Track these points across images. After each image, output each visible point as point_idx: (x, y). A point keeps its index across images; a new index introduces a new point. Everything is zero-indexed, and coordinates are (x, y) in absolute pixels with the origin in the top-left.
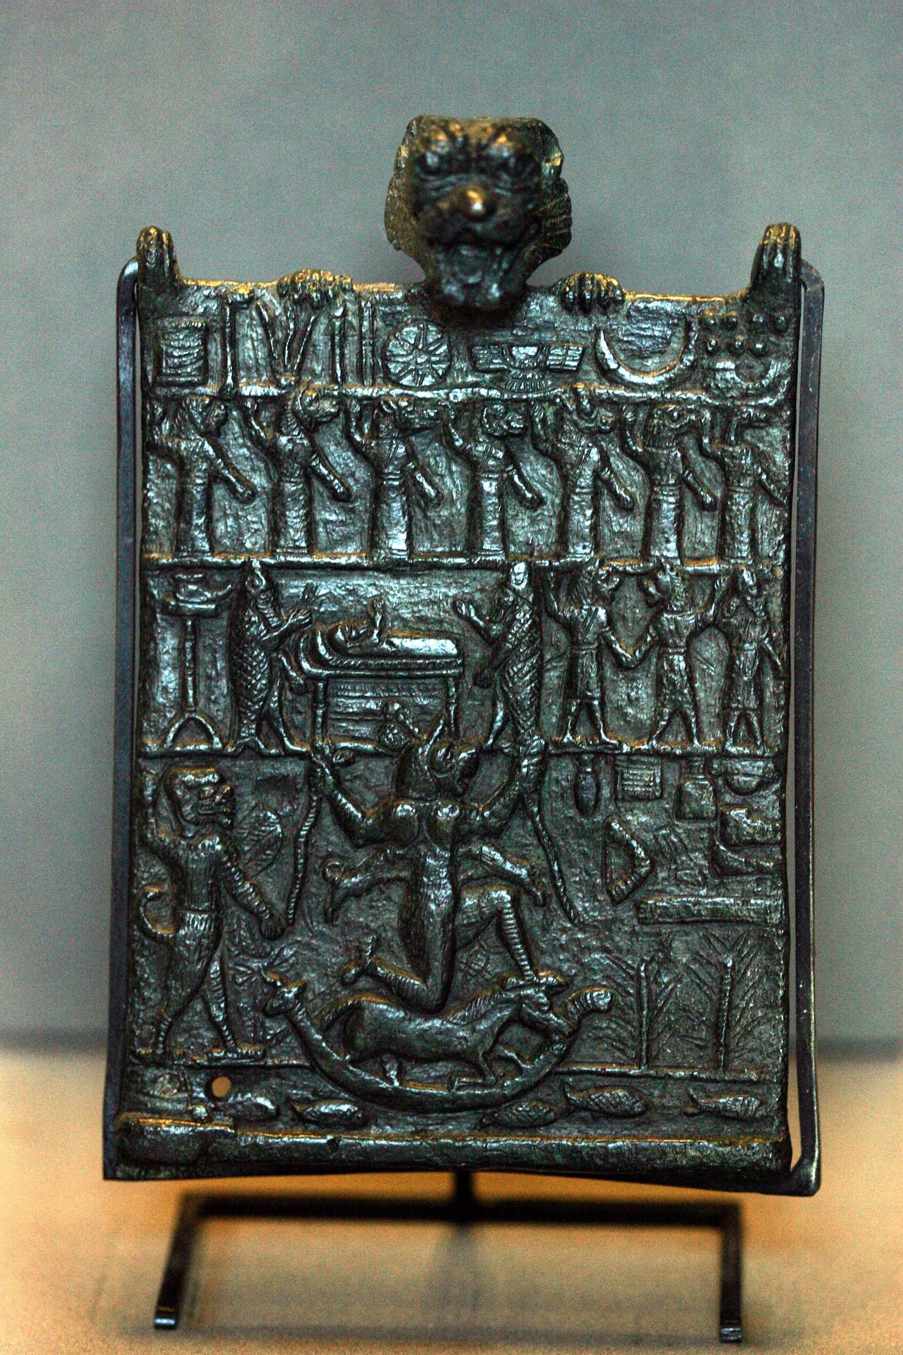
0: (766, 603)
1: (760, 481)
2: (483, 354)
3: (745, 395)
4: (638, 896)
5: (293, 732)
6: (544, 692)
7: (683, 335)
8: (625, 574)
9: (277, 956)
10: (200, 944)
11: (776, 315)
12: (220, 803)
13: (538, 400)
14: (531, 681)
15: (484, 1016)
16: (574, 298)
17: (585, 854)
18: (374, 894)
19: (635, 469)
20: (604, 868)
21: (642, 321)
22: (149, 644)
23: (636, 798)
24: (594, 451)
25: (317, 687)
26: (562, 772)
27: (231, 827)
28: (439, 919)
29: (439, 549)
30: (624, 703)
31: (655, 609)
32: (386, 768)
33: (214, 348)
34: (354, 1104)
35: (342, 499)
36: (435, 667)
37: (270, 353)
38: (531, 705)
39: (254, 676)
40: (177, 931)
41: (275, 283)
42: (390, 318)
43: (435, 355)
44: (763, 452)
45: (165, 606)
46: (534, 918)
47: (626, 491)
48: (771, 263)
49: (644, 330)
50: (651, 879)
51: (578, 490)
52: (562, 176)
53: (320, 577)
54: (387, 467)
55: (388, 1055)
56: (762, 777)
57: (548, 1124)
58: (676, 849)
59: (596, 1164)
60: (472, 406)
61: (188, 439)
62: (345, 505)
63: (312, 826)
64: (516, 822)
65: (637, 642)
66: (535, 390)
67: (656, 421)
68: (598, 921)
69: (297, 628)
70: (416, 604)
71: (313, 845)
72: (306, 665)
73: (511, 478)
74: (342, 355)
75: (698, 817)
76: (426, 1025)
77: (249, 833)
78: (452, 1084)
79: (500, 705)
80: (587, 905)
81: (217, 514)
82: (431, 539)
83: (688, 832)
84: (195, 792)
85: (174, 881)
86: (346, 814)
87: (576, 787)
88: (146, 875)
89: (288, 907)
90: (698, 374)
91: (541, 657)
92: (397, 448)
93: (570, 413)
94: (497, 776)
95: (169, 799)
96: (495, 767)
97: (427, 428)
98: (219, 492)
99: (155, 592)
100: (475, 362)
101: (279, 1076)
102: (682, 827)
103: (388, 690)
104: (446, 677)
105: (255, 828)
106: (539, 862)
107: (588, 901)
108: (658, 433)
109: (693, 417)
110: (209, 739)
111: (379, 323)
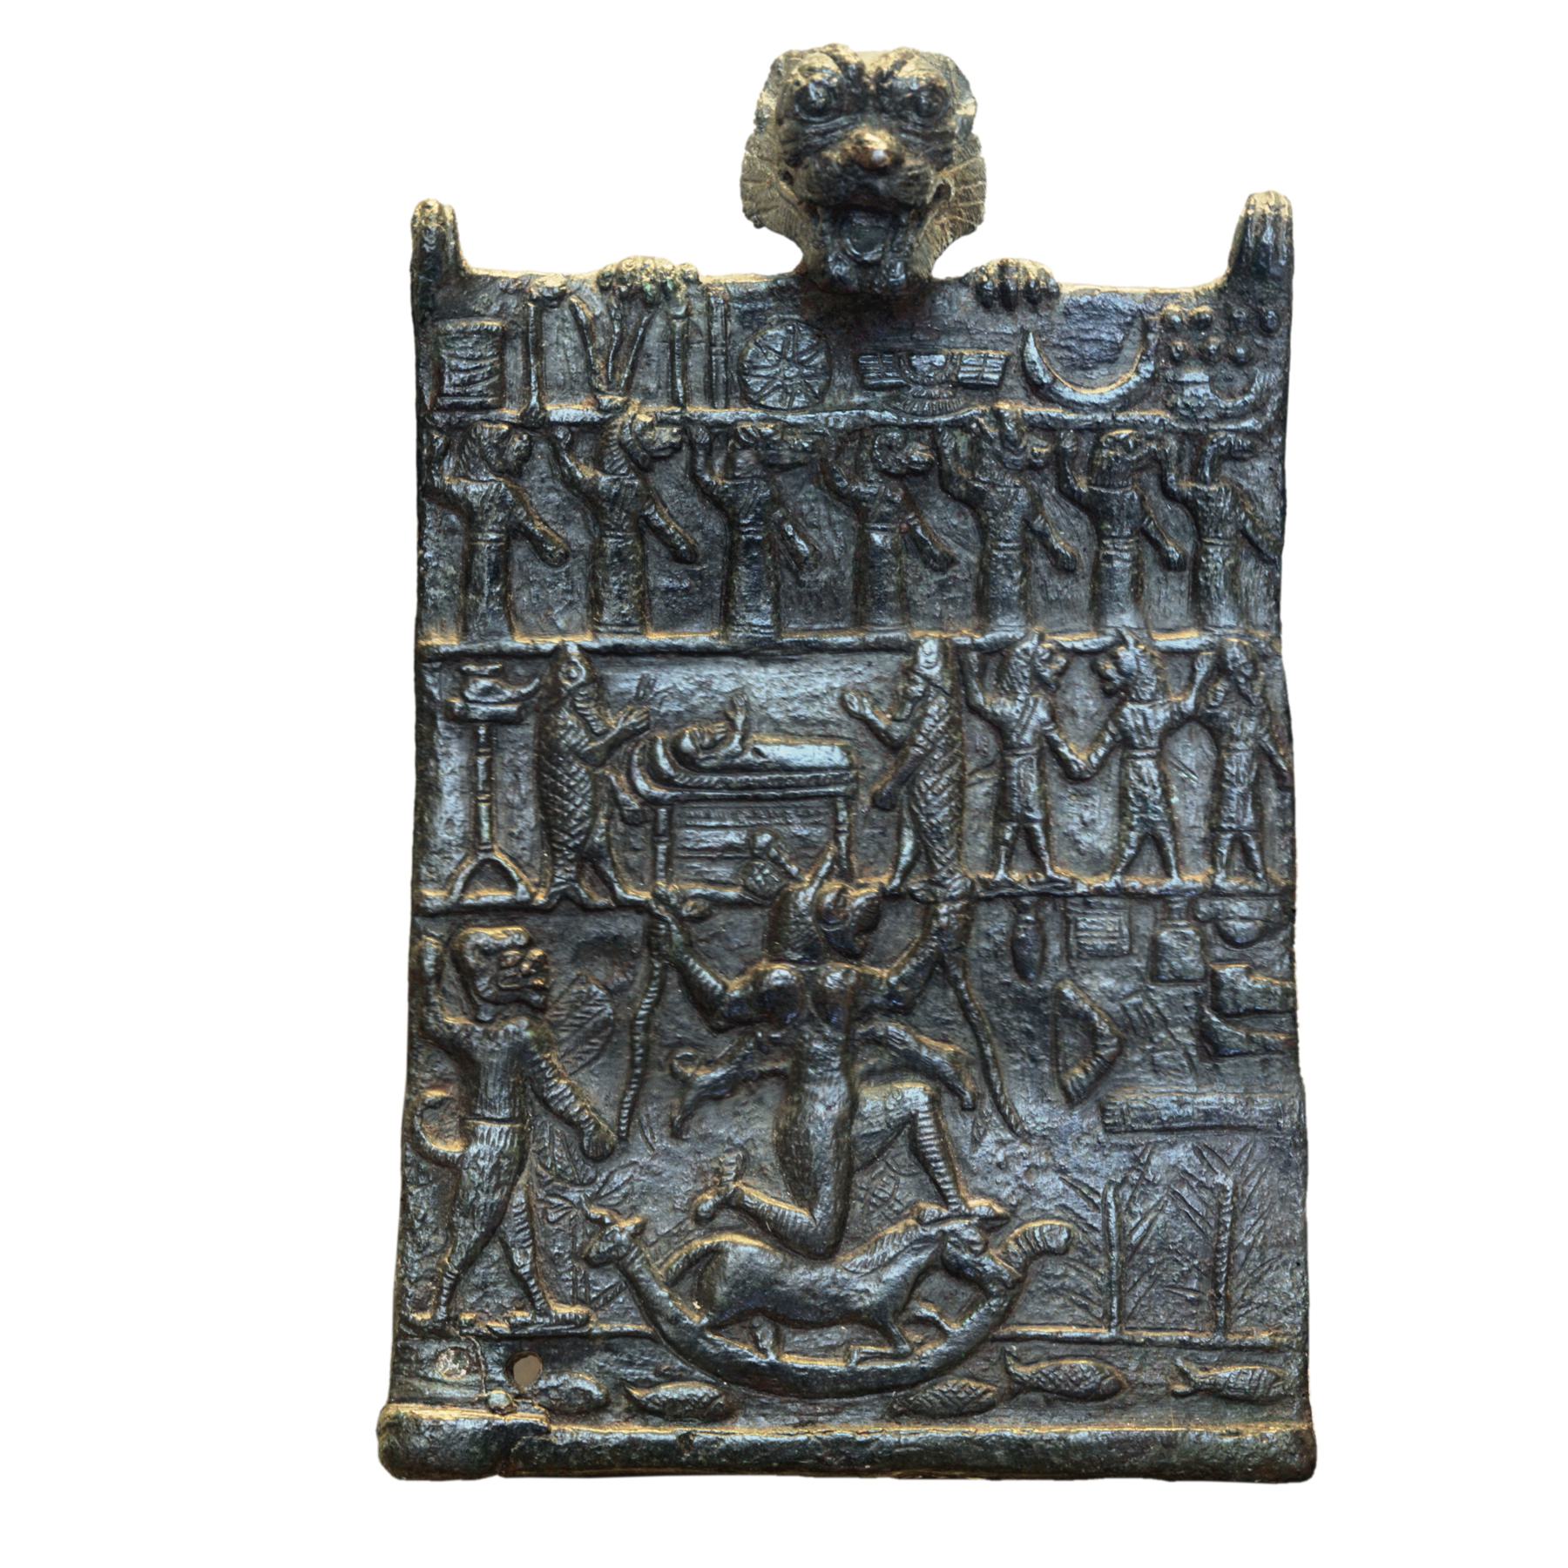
2: (873, 368)
3: (1223, 417)
4: (1102, 1092)
6: (966, 815)
7: (1138, 338)
8: (1076, 652)
9: (605, 1182)
10: (497, 1166)
12: (528, 975)
13: (946, 424)
14: (950, 799)
15: (893, 1260)
17: (1028, 1033)
18: (742, 1095)
20: (1054, 1050)
21: (1083, 321)
22: (426, 761)
23: (1098, 955)
24: (1022, 492)
25: (656, 814)
26: (995, 923)
28: (830, 1126)
29: (817, 626)
30: (1075, 828)
31: (1115, 699)
32: (755, 921)
33: (514, 359)
34: (715, 1385)
36: (819, 783)
38: (951, 832)
39: (571, 801)
42: (748, 318)
43: (808, 367)
46: (959, 1127)
49: (1087, 331)
53: (660, 666)
55: (761, 1319)
56: (1265, 921)
58: (1152, 1022)
59: (1052, 1463)
60: (860, 432)
62: (689, 568)
63: (657, 1003)
64: (935, 990)
66: (943, 412)
69: (630, 735)
70: (791, 700)
71: (656, 1029)
72: (642, 785)
74: (685, 369)
75: (1179, 979)
76: (815, 1275)
77: (568, 1016)
78: (850, 1357)
79: (908, 833)
83: (1169, 1000)
84: (494, 960)
86: (701, 985)
87: (1015, 943)
89: (620, 1117)
90: (1157, 388)
91: (963, 768)
93: (991, 441)
94: (905, 930)
95: (458, 969)
96: (903, 918)
97: (800, 464)
98: (520, 552)
99: (435, 691)
100: (863, 378)
101: (608, 1349)
102: (1162, 994)
103: (755, 816)
104: (836, 795)
105: (577, 1008)
108: (1109, 468)
110: (512, 885)
111: (733, 325)
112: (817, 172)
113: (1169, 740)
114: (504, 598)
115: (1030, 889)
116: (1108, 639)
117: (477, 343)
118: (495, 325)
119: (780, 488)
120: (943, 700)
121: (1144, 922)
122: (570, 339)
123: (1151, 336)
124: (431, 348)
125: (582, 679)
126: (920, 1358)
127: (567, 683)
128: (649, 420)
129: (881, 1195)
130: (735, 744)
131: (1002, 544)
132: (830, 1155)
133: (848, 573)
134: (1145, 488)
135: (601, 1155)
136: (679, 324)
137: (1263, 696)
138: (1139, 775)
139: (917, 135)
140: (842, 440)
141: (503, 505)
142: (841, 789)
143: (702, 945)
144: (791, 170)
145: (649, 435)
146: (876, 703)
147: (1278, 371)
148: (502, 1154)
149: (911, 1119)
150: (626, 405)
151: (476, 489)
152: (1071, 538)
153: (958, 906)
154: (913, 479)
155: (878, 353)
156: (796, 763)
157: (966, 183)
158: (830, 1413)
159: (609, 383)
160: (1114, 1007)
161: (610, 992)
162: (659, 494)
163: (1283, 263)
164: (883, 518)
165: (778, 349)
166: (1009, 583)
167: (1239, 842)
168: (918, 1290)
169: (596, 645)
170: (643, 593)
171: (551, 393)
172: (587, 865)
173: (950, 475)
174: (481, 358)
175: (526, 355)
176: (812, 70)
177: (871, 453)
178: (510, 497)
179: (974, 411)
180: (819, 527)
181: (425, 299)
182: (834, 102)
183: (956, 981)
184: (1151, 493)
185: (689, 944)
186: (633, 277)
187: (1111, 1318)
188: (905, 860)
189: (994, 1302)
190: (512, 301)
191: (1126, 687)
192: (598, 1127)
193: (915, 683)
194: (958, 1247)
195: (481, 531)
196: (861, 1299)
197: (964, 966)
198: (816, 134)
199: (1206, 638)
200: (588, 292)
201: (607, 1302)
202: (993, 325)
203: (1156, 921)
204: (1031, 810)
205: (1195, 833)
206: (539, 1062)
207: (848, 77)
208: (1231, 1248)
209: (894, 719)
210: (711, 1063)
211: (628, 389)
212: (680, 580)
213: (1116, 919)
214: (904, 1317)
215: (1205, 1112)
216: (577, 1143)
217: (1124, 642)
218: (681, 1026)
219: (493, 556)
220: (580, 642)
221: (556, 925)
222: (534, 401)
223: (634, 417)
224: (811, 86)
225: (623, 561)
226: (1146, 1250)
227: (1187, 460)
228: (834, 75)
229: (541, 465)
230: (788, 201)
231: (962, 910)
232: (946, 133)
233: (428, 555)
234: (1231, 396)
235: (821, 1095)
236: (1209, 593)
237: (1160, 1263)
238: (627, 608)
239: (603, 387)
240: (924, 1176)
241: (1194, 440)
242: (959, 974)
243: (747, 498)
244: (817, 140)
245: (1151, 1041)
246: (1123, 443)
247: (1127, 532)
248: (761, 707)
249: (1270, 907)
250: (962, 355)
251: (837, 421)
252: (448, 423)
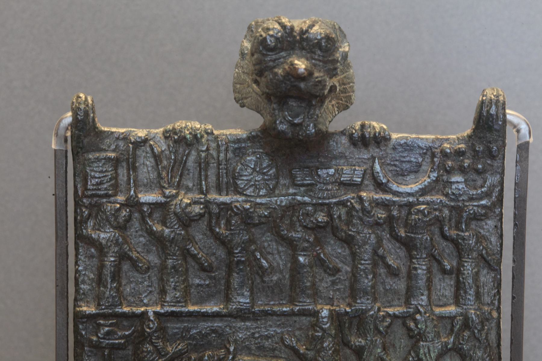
0: (487, 334)
1: (482, 255)
2: (299, 175)
3: (471, 199)
7: (429, 160)
8: (395, 317)
13: (335, 203)
19: (400, 248)
21: (402, 152)
24: (373, 236)
29: (272, 303)
31: (414, 340)
33: (122, 172)
41: (162, 130)
43: (267, 175)
44: (483, 236)
45: (91, 341)
60: (293, 207)
62: (209, 274)
66: (334, 197)
67: (413, 217)
74: (206, 176)
93: (357, 211)
97: (263, 223)
98: (126, 267)
99: (84, 333)
108: (415, 224)
109: (437, 213)
111: (230, 155)
112: (271, 79)
114: (118, 289)
117: (104, 164)
118: (113, 155)
119: (253, 235)
120: (331, 339)
122: (150, 162)
123: (436, 159)
124: (82, 167)
127: (148, 330)
128: (189, 201)
131: (363, 262)
133: (287, 276)
134: (433, 234)
136: (203, 155)
137: (486, 338)
139: (320, 61)
140: (284, 211)
141: (117, 244)
144: (258, 79)
145: (189, 209)
146: (298, 340)
147: (498, 176)
150: (177, 194)
151: (104, 236)
152: (397, 259)
155: (301, 168)
157: (344, 84)
159: (169, 183)
162: (194, 238)
163: (500, 123)
164: (304, 250)
165: (252, 166)
166: (366, 281)
169: (162, 311)
170: (186, 287)
171: (140, 189)
173: (337, 228)
174: (106, 171)
175: (128, 170)
176: (268, 29)
177: (298, 217)
178: (121, 240)
179: (349, 196)
180: (273, 254)
181: (78, 143)
182: (279, 45)
184: (436, 236)
186: (181, 132)
190: (121, 143)
195: (106, 257)
198: (270, 60)
199: (459, 310)
200: (158, 139)
202: (358, 154)
207: (286, 33)
209: (307, 349)
211: (179, 186)
212: (205, 280)
219: (112, 269)
220: (153, 310)
222: (132, 192)
223: (181, 200)
224: (268, 37)
225: (177, 271)
227: (454, 220)
228: (279, 32)
229: (136, 224)
230: (257, 94)
232: (334, 60)
233: (80, 268)
234: (475, 188)
236: (465, 286)
238: (178, 294)
239: (166, 186)
241: (457, 210)
243: (237, 240)
244: (271, 64)
246: (422, 212)
247: (424, 256)
250: (343, 169)
251: (281, 202)
252: (90, 204)
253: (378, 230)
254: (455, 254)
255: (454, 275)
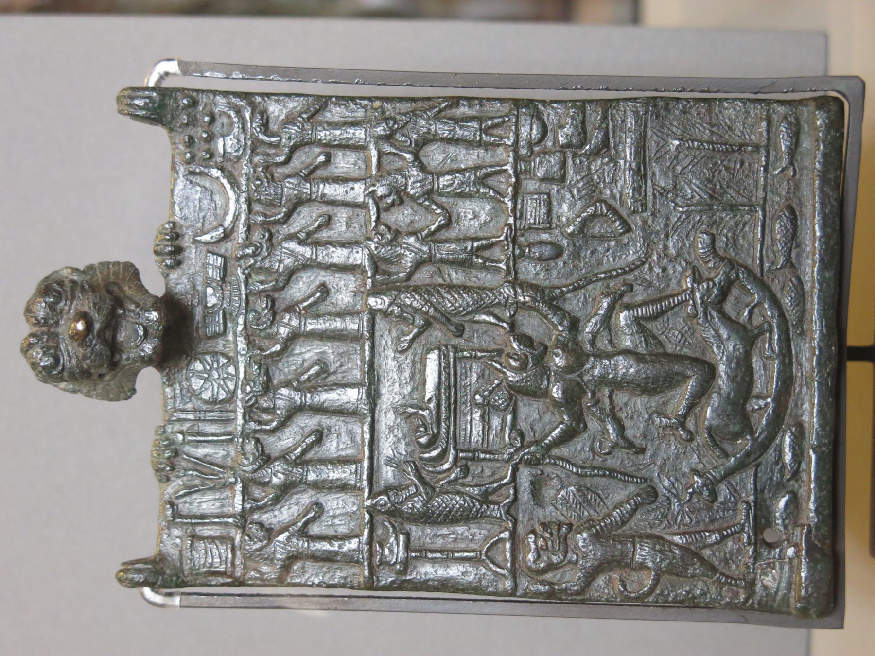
1: (309, 118)
4: (624, 213)
5: (497, 476)
6: (468, 284)
10: (660, 551)
11: (182, 105)
12: (551, 534)
13: (246, 286)
14: (459, 293)
15: (717, 332)
16: (171, 259)
17: (592, 253)
18: (622, 415)
19: (299, 214)
20: (602, 238)
23: (549, 212)
24: (285, 245)
25: (462, 458)
26: (530, 271)
27: (570, 526)
29: (359, 363)
30: (477, 223)
31: (405, 198)
32: (525, 405)
33: (206, 531)
34: (785, 432)
35: (320, 436)
37: (210, 489)
38: (477, 293)
40: (649, 568)
44: (286, 117)
47: (316, 220)
48: (141, 108)
49: (195, 206)
50: (611, 202)
51: (314, 257)
52: (82, 268)
53: (379, 454)
54: (295, 402)
55: (747, 406)
57: (800, 282)
61: (274, 553)
62: (325, 435)
63: (569, 462)
65: (430, 213)
67: (262, 197)
68: (644, 244)
72: (446, 466)
73: (304, 308)
74: (213, 435)
75: (563, 165)
80: (631, 252)
81: (331, 532)
82: (351, 369)
84: (542, 553)
85: (611, 570)
86: (560, 436)
88: (606, 591)
89: (632, 482)
91: (441, 285)
92: (282, 395)
94: (532, 320)
99: (390, 579)
100: (218, 334)
101: (762, 491)
103: (465, 403)
106: (598, 289)
107: (628, 251)
109: (260, 169)
110: (502, 540)
113: (429, 168)
115: (511, 249)
116: (371, 201)
119: (281, 383)
121: (531, 185)
125: (386, 498)
126: (772, 317)
129: (679, 337)
130: (425, 413)
132: (658, 366)
135: (653, 493)
137: (405, 114)
138: (448, 186)
142: (452, 355)
143: (537, 435)
148: (654, 549)
149: (637, 320)
153: (519, 291)
154: (276, 306)
155: (205, 326)
156: (436, 380)
158: (801, 369)
160: (579, 205)
161: (562, 488)
167: (486, 131)
168: (733, 318)
172: (490, 498)
183: (562, 293)
185: (536, 442)
187: (751, 210)
188: (493, 320)
189: (741, 276)
191: (398, 193)
192: (638, 495)
193: (392, 311)
194: (711, 295)
196: (738, 350)
197: (554, 287)
199: (372, 146)
201: (736, 490)
203: (531, 179)
204: (466, 248)
205: (481, 155)
206: (601, 527)
208: (712, 143)
209: (413, 324)
210: (605, 431)
213: (530, 201)
214: (748, 326)
215: (635, 155)
216: (647, 507)
217: (374, 192)
218: (583, 448)
221: (524, 517)
226: (713, 190)
229: (265, 517)
231: (522, 288)
235: (624, 371)
237: (720, 181)
240: (669, 313)
242: (557, 291)
245: (598, 183)
248: (404, 398)
249: (525, 113)
253: (277, 237)
254: (307, 149)
255: (332, 151)
